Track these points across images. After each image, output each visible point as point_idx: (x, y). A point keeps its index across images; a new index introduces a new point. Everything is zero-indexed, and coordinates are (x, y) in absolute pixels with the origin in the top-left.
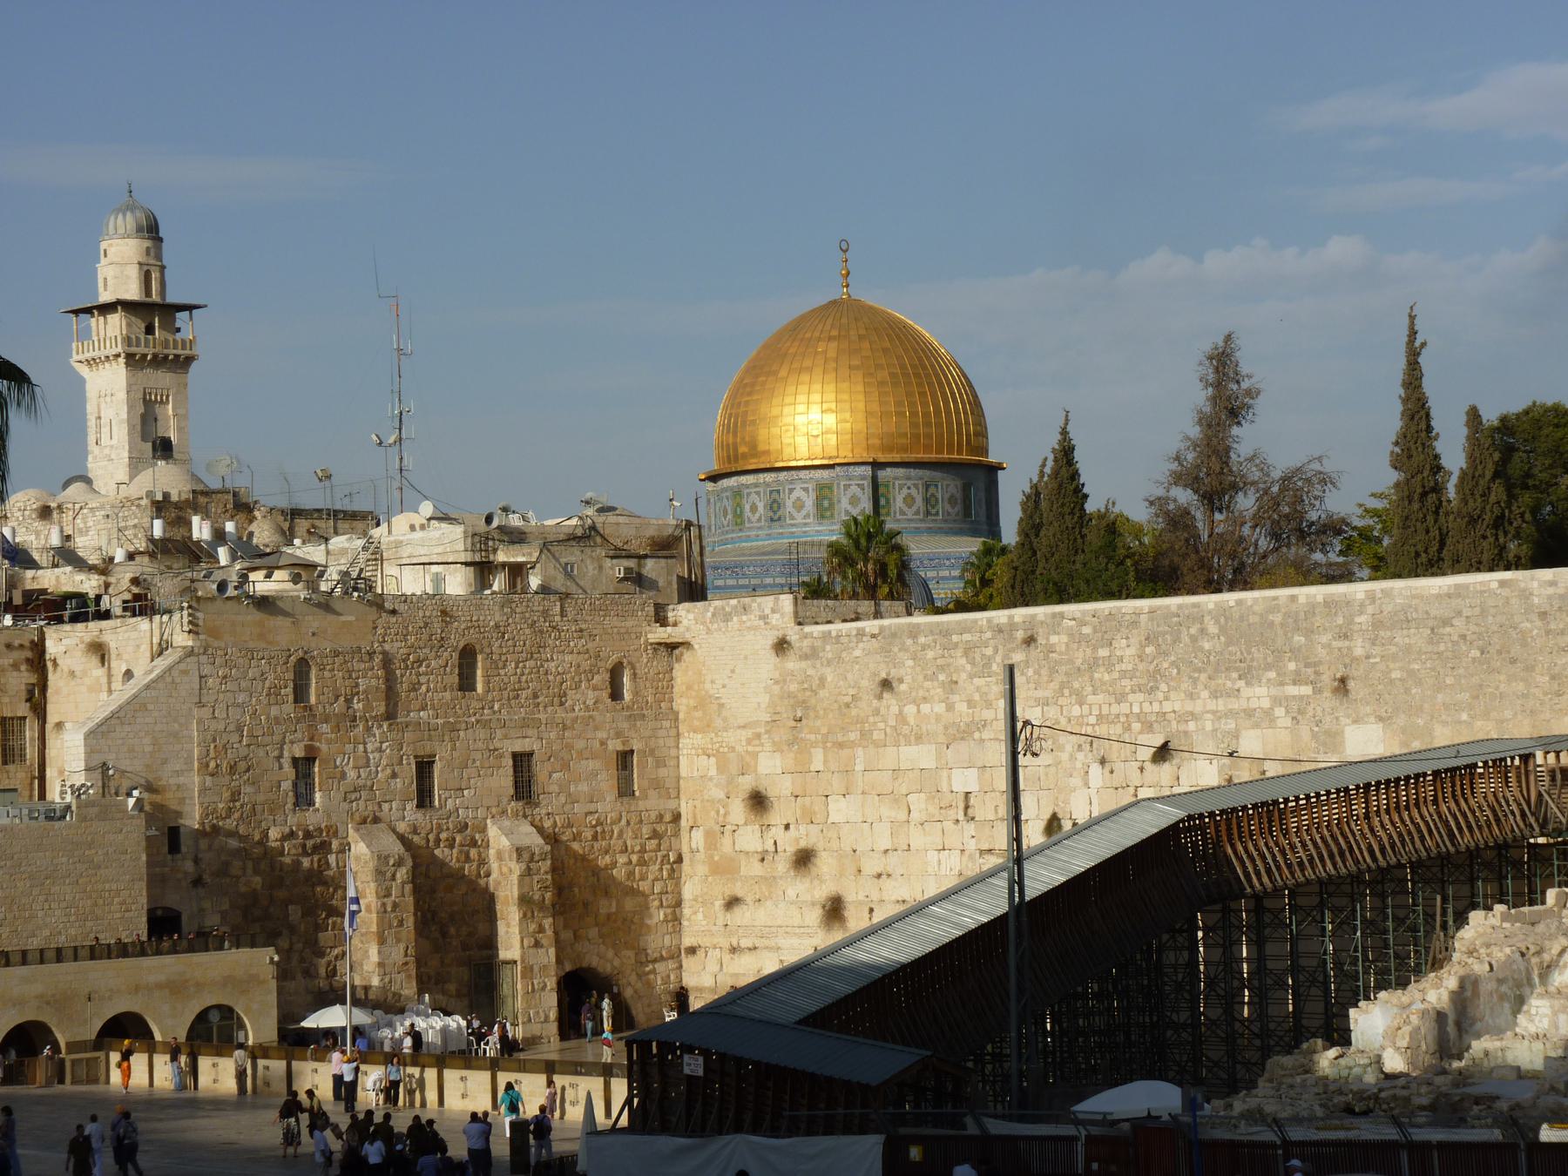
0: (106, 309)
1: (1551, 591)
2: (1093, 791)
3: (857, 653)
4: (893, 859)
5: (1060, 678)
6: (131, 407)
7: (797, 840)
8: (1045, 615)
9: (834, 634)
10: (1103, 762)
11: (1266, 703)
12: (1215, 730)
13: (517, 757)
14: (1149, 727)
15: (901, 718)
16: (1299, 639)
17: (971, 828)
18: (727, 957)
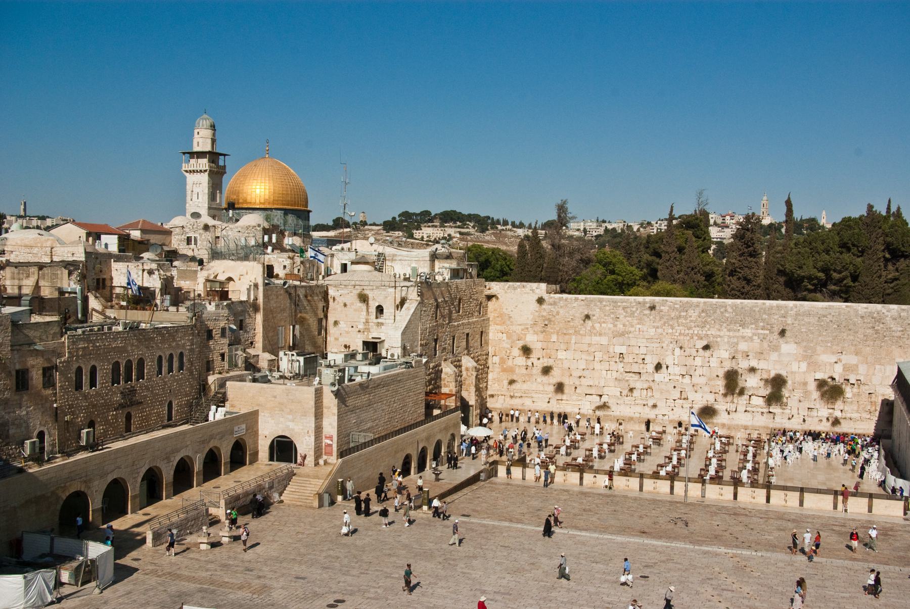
0: (200, 155)
1: (866, 310)
2: (676, 357)
3: (574, 305)
4: (586, 373)
5: (665, 320)
6: (209, 189)
7: (543, 363)
8: (660, 300)
9: (564, 298)
10: (681, 348)
11: (750, 335)
12: (728, 342)
13: (468, 335)
14: (701, 339)
15: (593, 327)
16: (765, 316)
17: (622, 365)
18: (508, 399)
